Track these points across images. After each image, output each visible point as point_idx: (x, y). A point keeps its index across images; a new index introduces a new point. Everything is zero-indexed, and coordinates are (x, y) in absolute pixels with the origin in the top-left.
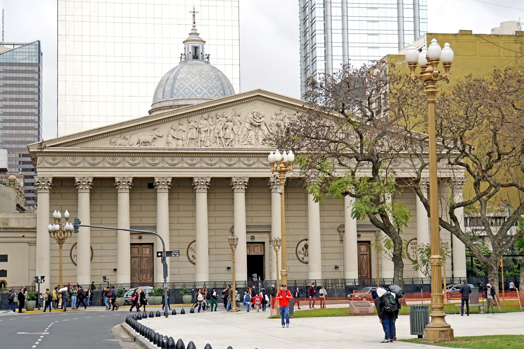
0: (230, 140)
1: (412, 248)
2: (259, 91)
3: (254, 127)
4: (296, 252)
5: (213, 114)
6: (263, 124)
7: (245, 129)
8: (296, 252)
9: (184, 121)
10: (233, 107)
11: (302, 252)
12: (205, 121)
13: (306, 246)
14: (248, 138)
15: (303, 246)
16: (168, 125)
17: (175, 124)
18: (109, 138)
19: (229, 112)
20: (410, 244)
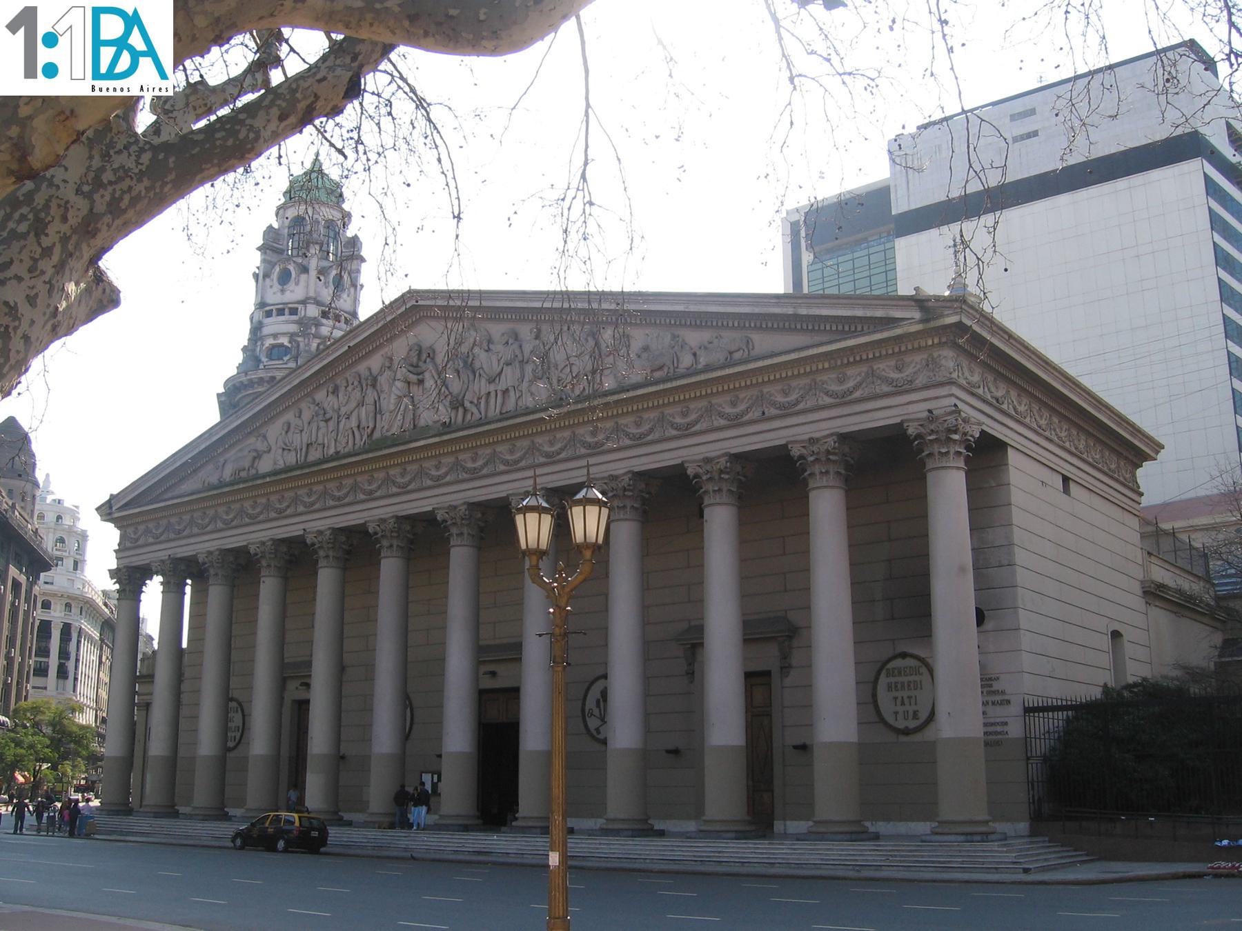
0: (369, 430)
1: (889, 688)
2: (412, 293)
3: (414, 389)
4: (583, 710)
5: (348, 374)
6: (427, 375)
7: (393, 397)
8: (583, 710)
9: (303, 405)
10: (382, 352)
11: (596, 712)
12: (331, 397)
13: (604, 694)
14: (399, 417)
15: (599, 696)
16: (278, 425)
17: (290, 416)
18: (200, 475)
19: (375, 362)
20: (884, 672)
